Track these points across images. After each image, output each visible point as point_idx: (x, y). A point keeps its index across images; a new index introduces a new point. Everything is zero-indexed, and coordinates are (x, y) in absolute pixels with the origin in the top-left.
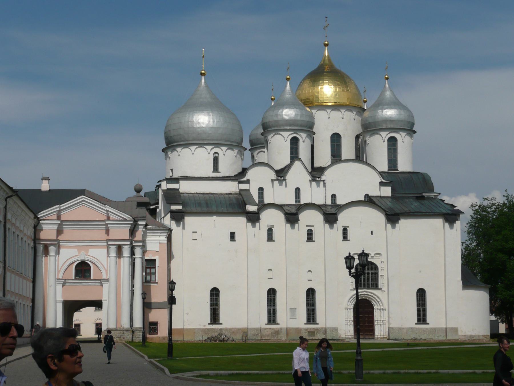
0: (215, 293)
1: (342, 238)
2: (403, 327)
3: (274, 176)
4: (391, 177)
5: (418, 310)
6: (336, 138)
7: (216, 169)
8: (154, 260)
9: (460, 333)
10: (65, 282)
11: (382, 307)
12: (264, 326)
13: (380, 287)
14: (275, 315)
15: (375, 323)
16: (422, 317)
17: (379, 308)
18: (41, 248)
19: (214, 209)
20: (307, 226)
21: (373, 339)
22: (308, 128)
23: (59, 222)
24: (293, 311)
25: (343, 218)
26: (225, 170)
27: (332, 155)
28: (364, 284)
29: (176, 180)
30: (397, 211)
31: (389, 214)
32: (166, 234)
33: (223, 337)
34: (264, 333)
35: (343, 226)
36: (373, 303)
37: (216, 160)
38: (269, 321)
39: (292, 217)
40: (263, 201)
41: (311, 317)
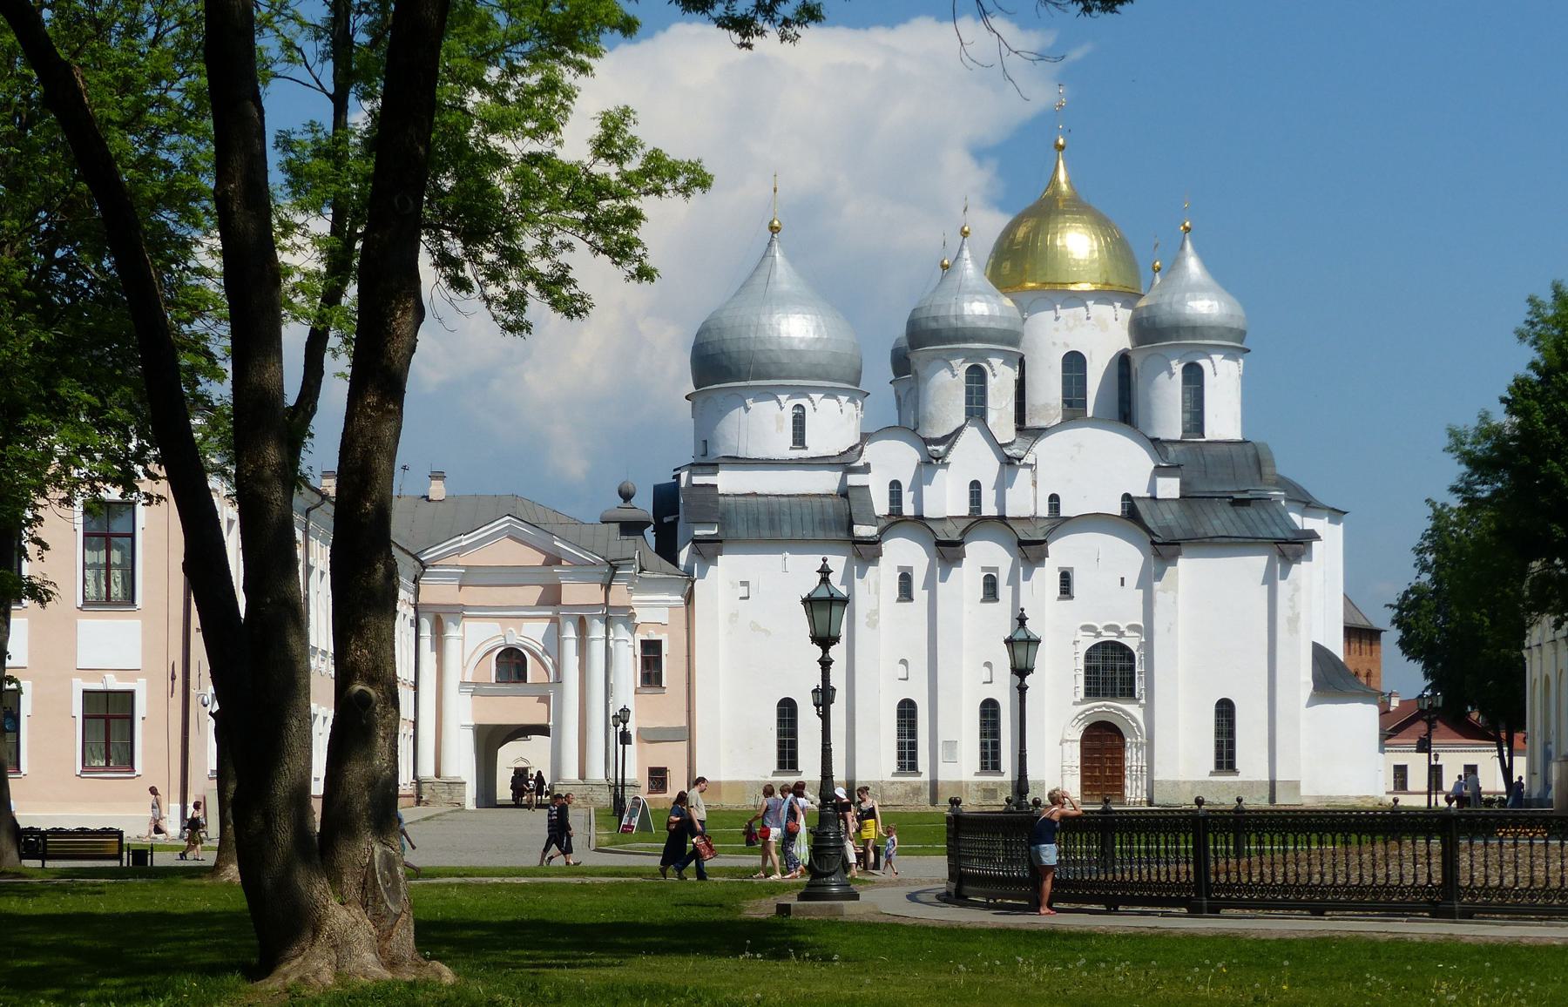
4: (1185, 455)
6: (1074, 364)
7: (799, 439)
9: (1304, 791)
10: (476, 689)
14: (913, 756)
16: (1225, 759)
18: (426, 625)
19: (786, 532)
20: (984, 569)
21: (1123, 804)
22: (1009, 343)
24: (951, 745)
25: (1061, 552)
26: (817, 445)
27: (1064, 401)
29: (713, 467)
30: (1178, 535)
31: (1159, 540)
37: (799, 423)
38: (901, 766)
39: (948, 551)
40: (900, 509)
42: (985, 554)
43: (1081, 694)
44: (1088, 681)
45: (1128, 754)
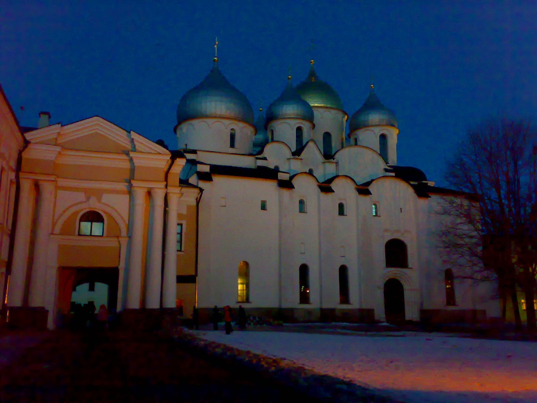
3: (289, 155)
6: (327, 136)
7: (232, 145)
15: (406, 304)
18: (26, 186)
20: (339, 199)
23: (58, 149)
36: (402, 282)
39: (326, 187)
42: (344, 190)
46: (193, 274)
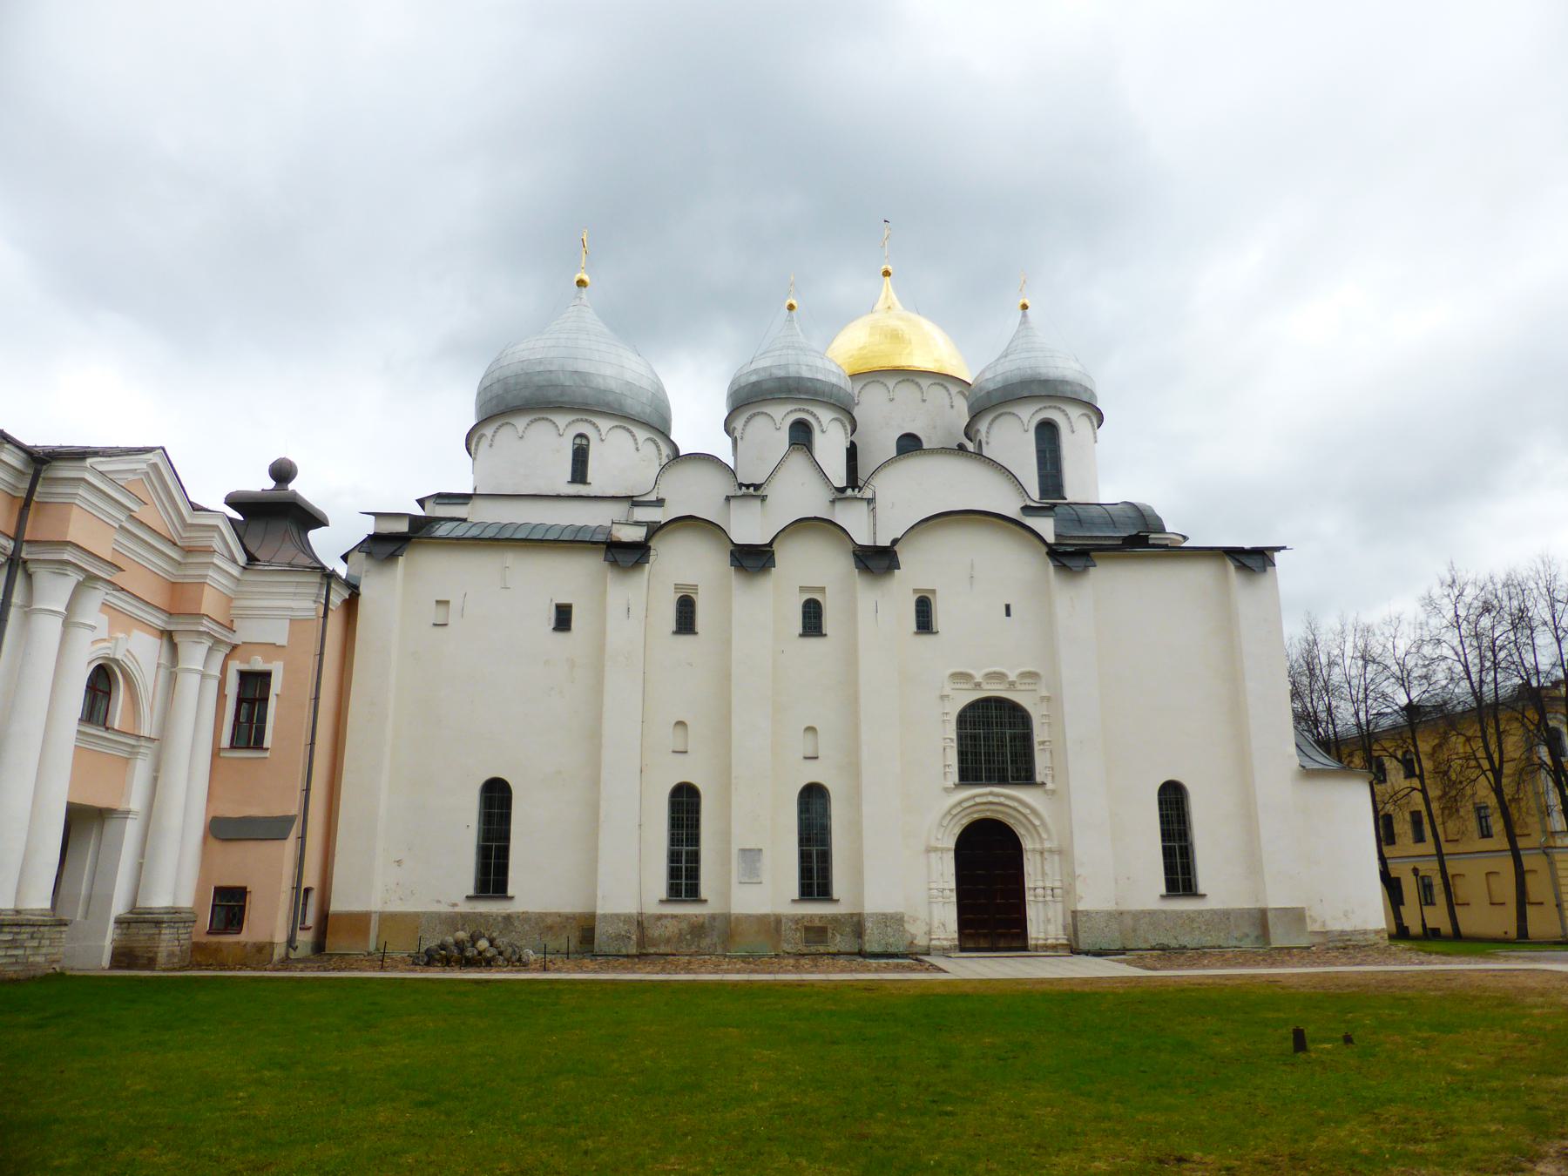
0: (496, 797)
1: (913, 626)
2: (1124, 907)
5: (1168, 853)
8: (267, 675)
9: (1311, 927)
11: (1047, 845)
12: (652, 908)
13: (1039, 779)
14: (694, 874)
15: (1029, 897)
17: (1038, 846)
20: (803, 589)
24: (751, 856)
28: (989, 770)
32: (315, 590)
33: (483, 944)
34: (655, 932)
35: (915, 591)
41: (815, 877)
43: (956, 778)
44: (962, 755)
45: (1029, 868)
46: (294, 809)
